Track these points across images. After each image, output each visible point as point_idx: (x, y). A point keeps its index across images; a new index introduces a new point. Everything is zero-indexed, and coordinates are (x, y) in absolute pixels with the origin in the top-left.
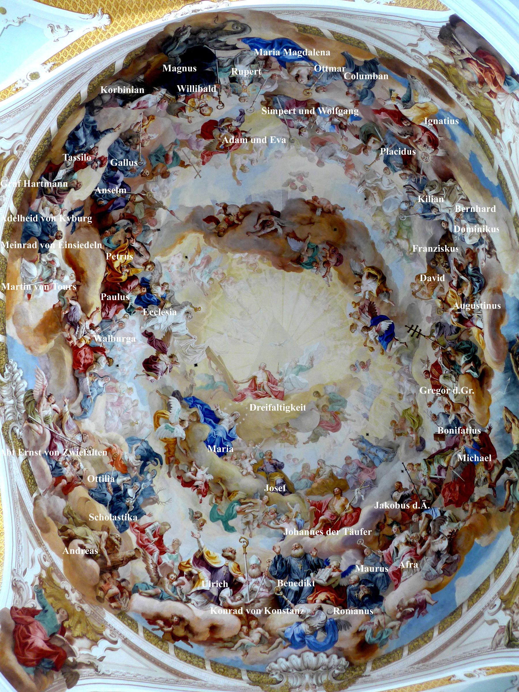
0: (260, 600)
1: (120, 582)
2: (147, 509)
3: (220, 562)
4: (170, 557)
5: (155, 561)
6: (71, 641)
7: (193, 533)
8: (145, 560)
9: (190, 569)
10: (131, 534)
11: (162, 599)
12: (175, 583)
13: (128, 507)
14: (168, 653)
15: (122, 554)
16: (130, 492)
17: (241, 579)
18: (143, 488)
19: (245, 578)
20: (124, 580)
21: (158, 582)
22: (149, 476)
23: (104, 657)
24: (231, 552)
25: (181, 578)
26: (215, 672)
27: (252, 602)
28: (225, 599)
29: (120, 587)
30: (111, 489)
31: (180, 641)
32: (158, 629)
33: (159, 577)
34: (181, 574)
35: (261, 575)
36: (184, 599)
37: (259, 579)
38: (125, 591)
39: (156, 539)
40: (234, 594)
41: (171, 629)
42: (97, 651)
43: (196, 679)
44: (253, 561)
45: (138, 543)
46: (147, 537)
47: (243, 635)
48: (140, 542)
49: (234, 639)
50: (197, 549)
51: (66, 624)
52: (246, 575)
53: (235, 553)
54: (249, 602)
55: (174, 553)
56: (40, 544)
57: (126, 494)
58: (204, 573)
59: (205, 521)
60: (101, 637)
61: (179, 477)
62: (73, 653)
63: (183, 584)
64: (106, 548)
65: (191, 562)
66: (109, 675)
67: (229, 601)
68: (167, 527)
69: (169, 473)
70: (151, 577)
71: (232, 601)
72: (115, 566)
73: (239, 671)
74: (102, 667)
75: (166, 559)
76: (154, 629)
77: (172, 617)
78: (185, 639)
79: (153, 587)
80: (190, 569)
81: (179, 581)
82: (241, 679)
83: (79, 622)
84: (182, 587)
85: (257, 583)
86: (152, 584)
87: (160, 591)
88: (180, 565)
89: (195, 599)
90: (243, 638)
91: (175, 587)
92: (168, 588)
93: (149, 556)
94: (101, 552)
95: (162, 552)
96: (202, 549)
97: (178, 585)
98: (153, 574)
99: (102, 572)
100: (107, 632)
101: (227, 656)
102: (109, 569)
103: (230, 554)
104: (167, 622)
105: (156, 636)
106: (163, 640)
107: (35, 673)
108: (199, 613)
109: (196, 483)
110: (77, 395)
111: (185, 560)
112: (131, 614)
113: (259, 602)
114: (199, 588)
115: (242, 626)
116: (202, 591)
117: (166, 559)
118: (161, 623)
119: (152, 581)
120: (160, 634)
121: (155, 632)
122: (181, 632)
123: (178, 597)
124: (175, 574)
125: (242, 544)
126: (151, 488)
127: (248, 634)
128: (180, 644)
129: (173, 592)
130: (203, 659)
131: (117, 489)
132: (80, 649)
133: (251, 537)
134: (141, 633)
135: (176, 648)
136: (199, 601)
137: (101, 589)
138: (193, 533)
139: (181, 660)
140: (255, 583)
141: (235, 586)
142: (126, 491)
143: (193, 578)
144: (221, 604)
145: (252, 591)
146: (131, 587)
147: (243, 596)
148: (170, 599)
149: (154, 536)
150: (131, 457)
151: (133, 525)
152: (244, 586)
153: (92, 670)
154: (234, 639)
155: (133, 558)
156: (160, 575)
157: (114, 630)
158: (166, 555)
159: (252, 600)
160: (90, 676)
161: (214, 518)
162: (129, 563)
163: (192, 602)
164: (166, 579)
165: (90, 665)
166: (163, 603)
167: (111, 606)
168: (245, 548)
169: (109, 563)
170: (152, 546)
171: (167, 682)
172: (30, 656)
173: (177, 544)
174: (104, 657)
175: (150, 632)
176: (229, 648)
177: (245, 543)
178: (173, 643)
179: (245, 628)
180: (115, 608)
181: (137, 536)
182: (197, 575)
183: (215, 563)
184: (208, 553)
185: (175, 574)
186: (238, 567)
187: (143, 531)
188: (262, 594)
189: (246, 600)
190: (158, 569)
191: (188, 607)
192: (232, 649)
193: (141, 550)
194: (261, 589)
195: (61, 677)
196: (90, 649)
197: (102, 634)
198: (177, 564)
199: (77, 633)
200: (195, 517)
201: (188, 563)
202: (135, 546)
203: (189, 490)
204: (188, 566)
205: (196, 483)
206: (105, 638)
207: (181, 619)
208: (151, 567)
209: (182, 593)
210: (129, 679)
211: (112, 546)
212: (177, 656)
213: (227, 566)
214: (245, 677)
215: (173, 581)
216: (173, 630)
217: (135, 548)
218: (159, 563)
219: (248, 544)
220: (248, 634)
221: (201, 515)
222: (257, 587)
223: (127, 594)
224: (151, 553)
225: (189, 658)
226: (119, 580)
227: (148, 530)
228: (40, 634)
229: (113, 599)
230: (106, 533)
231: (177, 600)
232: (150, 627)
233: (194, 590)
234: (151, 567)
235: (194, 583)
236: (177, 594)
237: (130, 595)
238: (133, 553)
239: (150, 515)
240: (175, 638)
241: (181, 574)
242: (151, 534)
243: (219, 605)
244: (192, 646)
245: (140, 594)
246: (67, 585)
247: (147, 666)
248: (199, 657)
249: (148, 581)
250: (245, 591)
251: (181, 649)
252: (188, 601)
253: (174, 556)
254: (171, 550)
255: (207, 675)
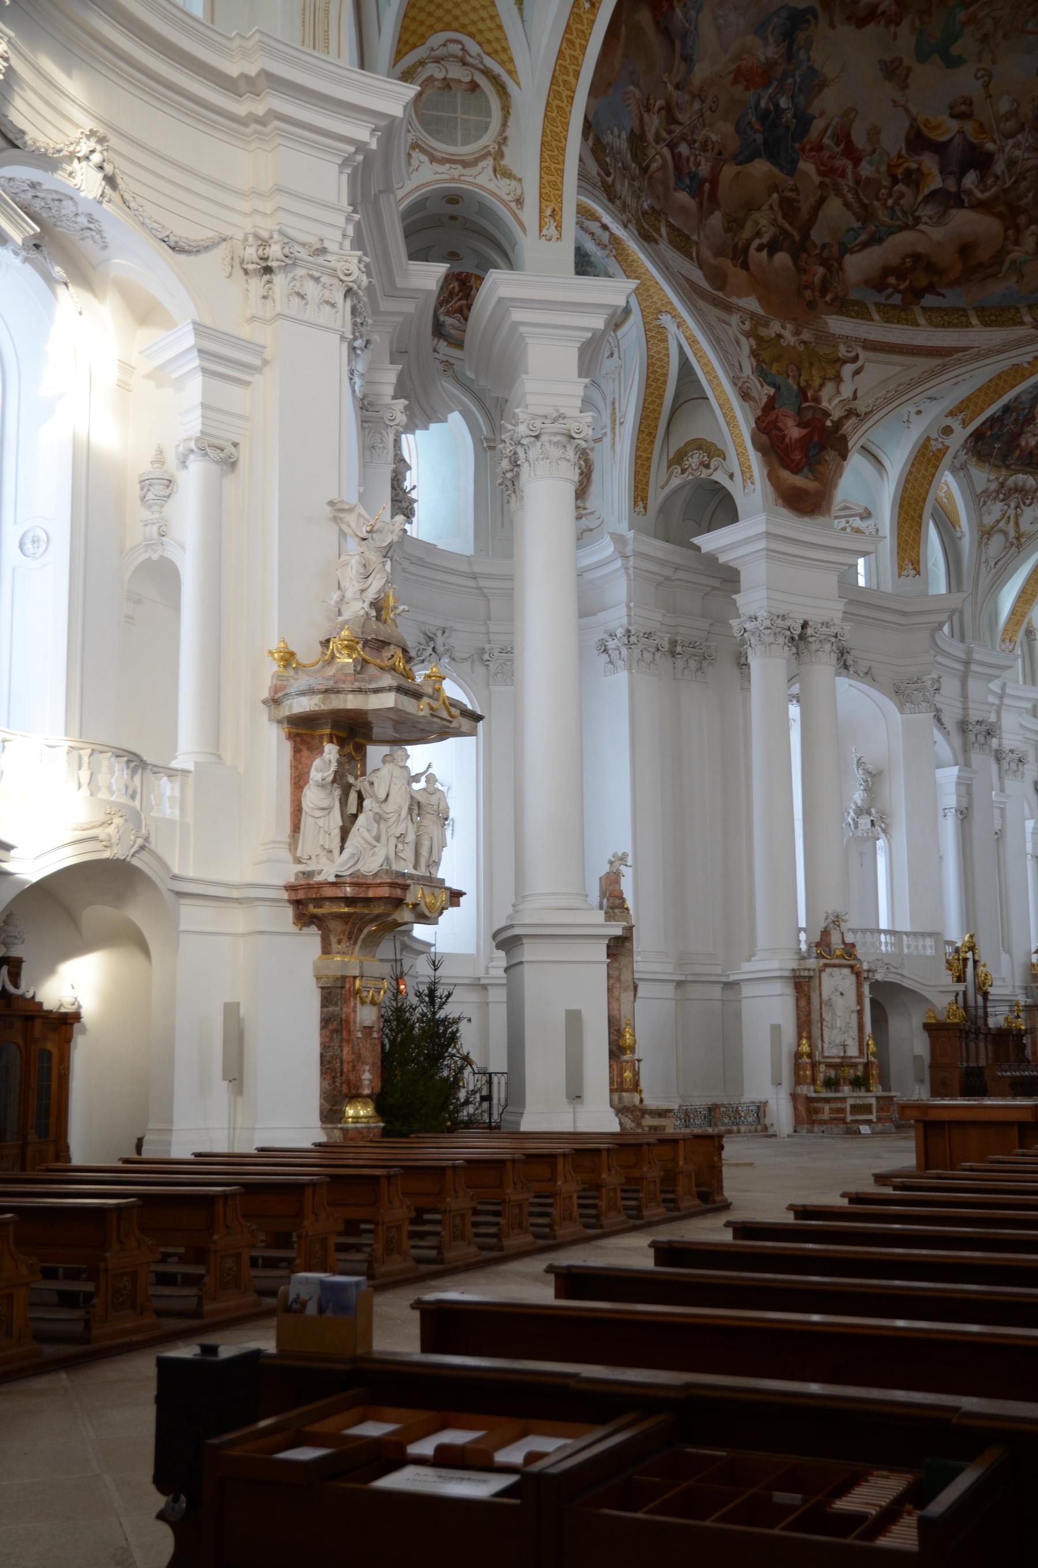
0: (1027, 175)
1: (820, 255)
2: (814, 109)
3: (948, 128)
4: (870, 164)
5: (851, 184)
6: (817, 400)
7: (894, 102)
8: (839, 193)
9: (905, 165)
10: (807, 167)
11: (880, 241)
12: (890, 202)
13: (788, 128)
14: (918, 325)
15: (805, 207)
16: (784, 102)
17: (990, 146)
18: (798, 80)
19: (994, 142)
20: (824, 246)
21: (866, 215)
22: (802, 55)
23: (856, 391)
24: (964, 103)
25: (896, 188)
26: (986, 325)
27: (1015, 182)
28: (970, 193)
29: (825, 263)
30: (758, 126)
31: (927, 296)
32: (892, 294)
33: (865, 207)
34: (895, 181)
35: (1022, 129)
36: (911, 222)
37: (1020, 137)
38: (833, 264)
39: (842, 146)
40: (982, 179)
41: (908, 282)
42: (846, 390)
43: (965, 349)
44: (1004, 107)
45: (820, 173)
46: (828, 154)
47: (1011, 247)
48: (822, 168)
49: (1000, 255)
50: (907, 124)
51: (803, 384)
52: (996, 136)
53: (971, 103)
54: (1009, 184)
55: (874, 152)
56: (728, 308)
57: (779, 111)
58: (929, 163)
59: (909, 69)
60: (839, 364)
61: (849, 18)
62: (827, 414)
63: (902, 195)
64: (784, 218)
65: (904, 152)
66: (871, 411)
67: (978, 194)
68: (852, 116)
69: (832, 25)
70: (854, 214)
71: (982, 192)
72: (806, 235)
73: (1017, 310)
74: (861, 406)
75: (866, 170)
76: (888, 297)
77: (903, 260)
78: (931, 289)
79: (864, 228)
80: (905, 165)
81: (895, 195)
82: (1022, 323)
83: (811, 365)
84: (902, 202)
85: (1017, 146)
86: (859, 224)
87: (874, 228)
88: (889, 166)
89: (926, 212)
90: (1013, 251)
91: (892, 208)
92: (883, 217)
93: (841, 181)
94: (783, 231)
95: (857, 162)
96: (915, 120)
97: (896, 202)
98: (856, 205)
99: (795, 259)
100: (842, 351)
101: (997, 290)
102: (799, 248)
103: (963, 108)
104: (900, 273)
105: (895, 307)
106: (905, 307)
107: (811, 470)
108: (937, 234)
109: (881, 9)
110: (673, 44)
111: (894, 154)
112: (853, 295)
113: (1025, 179)
114: (926, 192)
115: (1006, 230)
116: (934, 194)
117: (866, 170)
118: (892, 280)
119: (858, 220)
120: (897, 299)
121: (891, 301)
122: (923, 281)
123: (900, 223)
124: (886, 187)
125: (981, 81)
126: (812, 70)
127: (1017, 243)
128: (929, 300)
129: (892, 219)
130: (964, 310)
131: (764, 116)
132: (830, 401)
133: (994, 62)
134: (876, 316)
135: (924, 309)
136: (931, 213)
137: (806, 287)
138: (894, 102)
139: (937, 327)
140: (1014, 146)
141: (981, 161)
142: (777, 105)
143: (914, 178)
144: (966, 205)
145: (1012, 163)
146: (835, 250)
147: (997, 178)
148: (892, 233)
149: (838, 144)
150: (767, 51)
151: (803, 150)
152: (996, 157)
153: (853, 420)
154: (1000, 255)
155: (822, 201)
156: (866, 201)
157: (848, 340)
158: (864, 164)
159: (1013, 179)
160: (856, 428)
161: (922, 56)
162: (820, 214)
163: (924, 219)
164: (876, 203)
165: (851, 413)
166: (885, 244)
167: (826, 302)
168: (986, 86)
169: (797, 237)
170: (840, 163)
171: (933, 374)
172: (797, 456)
173: (874, 133)
174: (856, 391)
175: (885, 305)
176: (994, 276)
177: (986, 78)
178: (918, 304)
179: (1011, 232)
180: (833, 300)
181: (815, 163)
182: (919, 169)
183: (943, 134)
184: (927, 123)
185: (886, 187)
186: (981, 125)
187: (819, 147)
188: (1029, 164)
189: (1005, 182)
190: (861, 194)
191: (920, 231)
192: (1000, 275)
193: (828, 180)
194: (1026, 155)
195: (833, 453)
196: (838, 393)
197: (839, 359)
198: (883, 168)
199: (817, 383)
200: (894, 71)
201: (900, 156)
202: (817, 179)
203: (871, 28)
204: (901, 161)
205: (881, 9)
206: (844, 362)
207: (916, 257)
208: (850, 196)
209: (904, 213)
210: (892, 400)
211: (789, 207)
212: (931, 323)
213: (963, 132)
214: (1027, 319)
215: (886, 200)
216: (911, 281)
217: (817, 183)
218: (857, 182)
219: (990, 77)
220: (1017, 243)
221: (901, 61)
222: (1018, 153)
223: (836, 265)
224: (843, 175)
225: (946, 318)
226: (817, 252)
227: (826, 141)
228: (790, 423)
229: (824, 290)
230: (775, 195)
231: (901, 229)
232: (881, 298)
233: (920, 198)
234: (850, 196)
235: (918, 186)
236: (899, 219)
237: (840, 264)
238: (819, 193)
239: (822, 114)
240: (918, 294)
241: (895, 181)
242: (832, 144)
243: (963, 207)
244: (944, 296)
245: (852, 253)
246: (775, 327)
247: (902, 365)
248: (957, 310)
249: (856, 224)
250: (999, 167)
251: (931, 309)
252: (918, 220)
253: (876, 156)
254: (868, 148)
255: (979, 336)
